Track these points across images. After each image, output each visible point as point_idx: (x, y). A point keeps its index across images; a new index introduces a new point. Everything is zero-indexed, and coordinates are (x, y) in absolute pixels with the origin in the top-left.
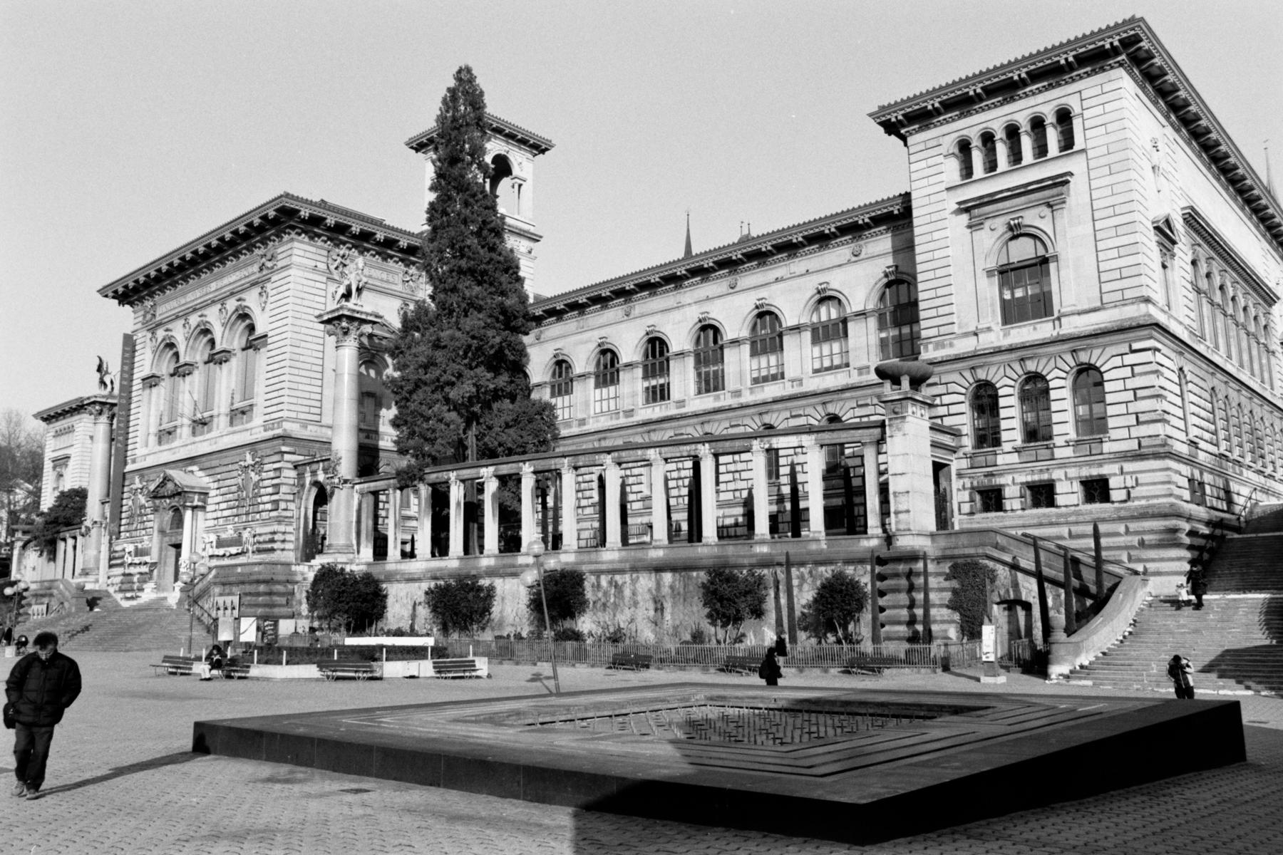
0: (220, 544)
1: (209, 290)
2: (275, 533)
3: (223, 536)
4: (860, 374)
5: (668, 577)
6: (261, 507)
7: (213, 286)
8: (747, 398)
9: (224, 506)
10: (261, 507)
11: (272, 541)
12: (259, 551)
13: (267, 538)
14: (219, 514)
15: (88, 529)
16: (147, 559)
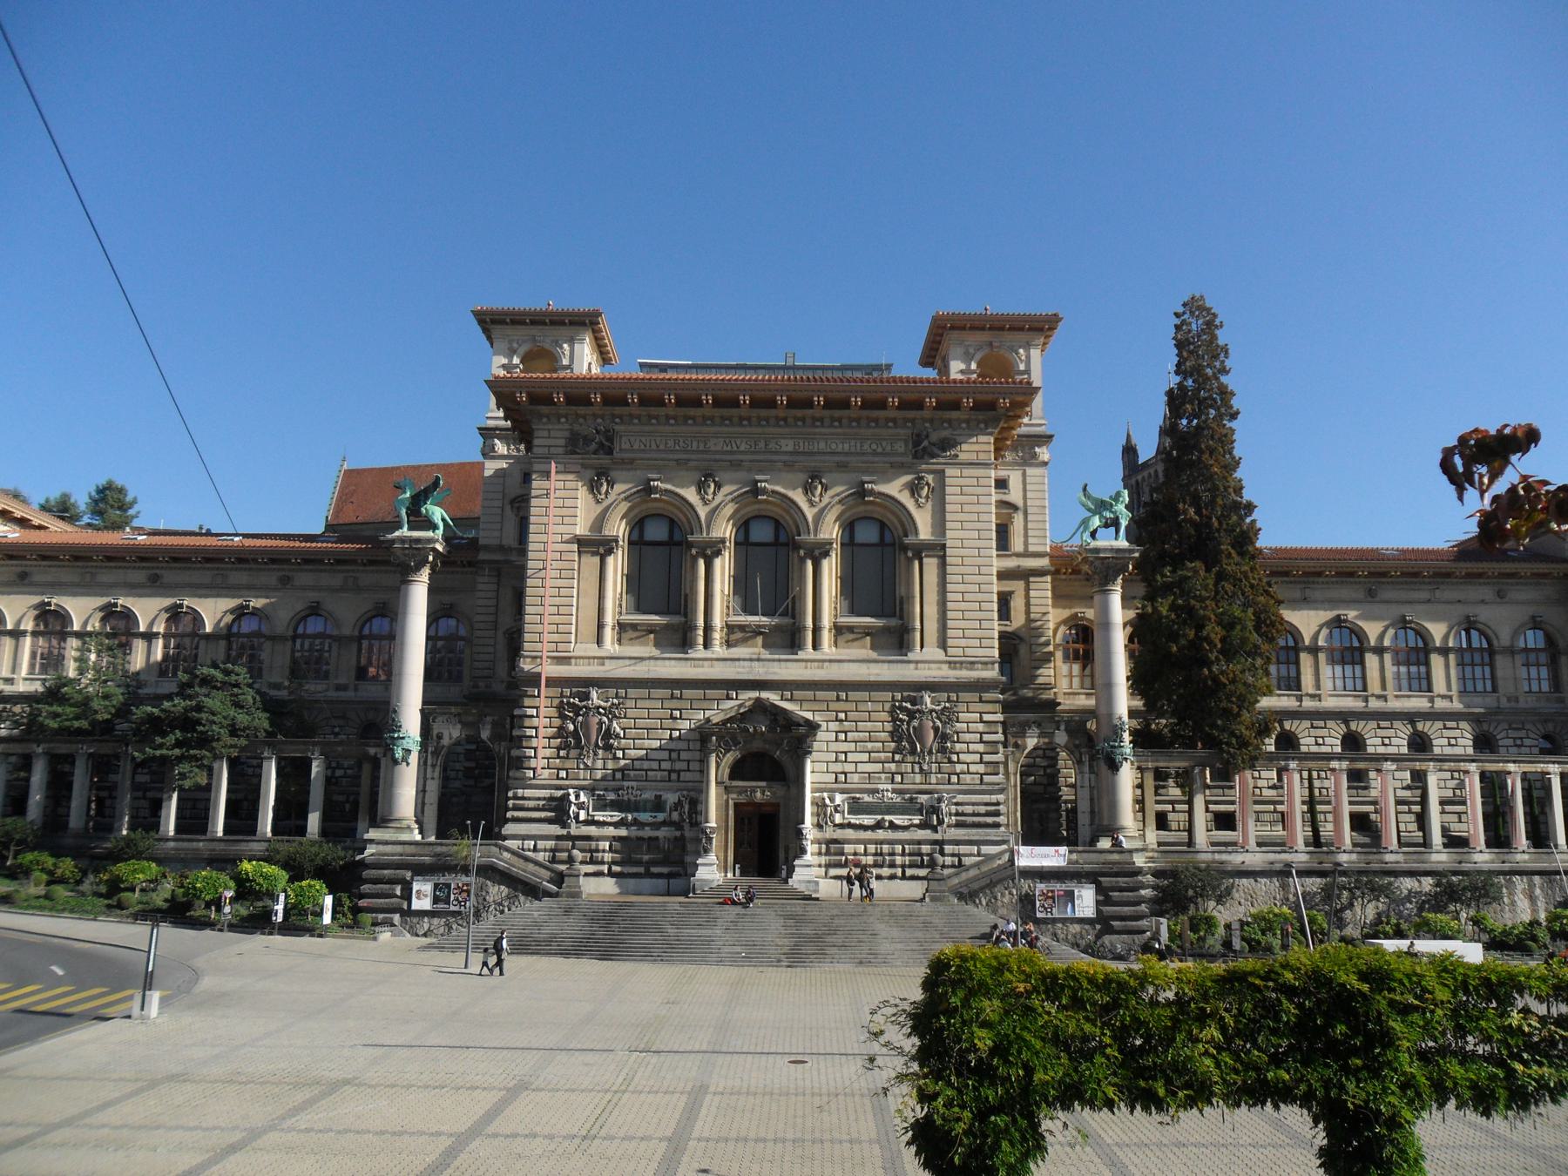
0: (856, 807)
1: (772, 446)
2: (998, 804)
3: (867, 798)
4: (1509, 700)
5: (1537, 879)
6: (959, 768)
7: (788, 445)
8: (1395, 704)
9: (865, 757)
10: (959, 768)
11: (997, 814)
12: (959, 825)
13: (983, 809)
14: (850, 768)
15: (408, 751)
16: (645, 817)
